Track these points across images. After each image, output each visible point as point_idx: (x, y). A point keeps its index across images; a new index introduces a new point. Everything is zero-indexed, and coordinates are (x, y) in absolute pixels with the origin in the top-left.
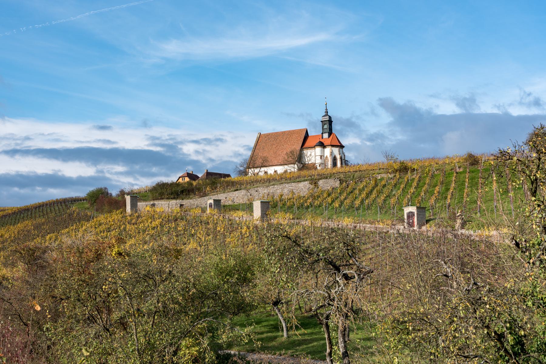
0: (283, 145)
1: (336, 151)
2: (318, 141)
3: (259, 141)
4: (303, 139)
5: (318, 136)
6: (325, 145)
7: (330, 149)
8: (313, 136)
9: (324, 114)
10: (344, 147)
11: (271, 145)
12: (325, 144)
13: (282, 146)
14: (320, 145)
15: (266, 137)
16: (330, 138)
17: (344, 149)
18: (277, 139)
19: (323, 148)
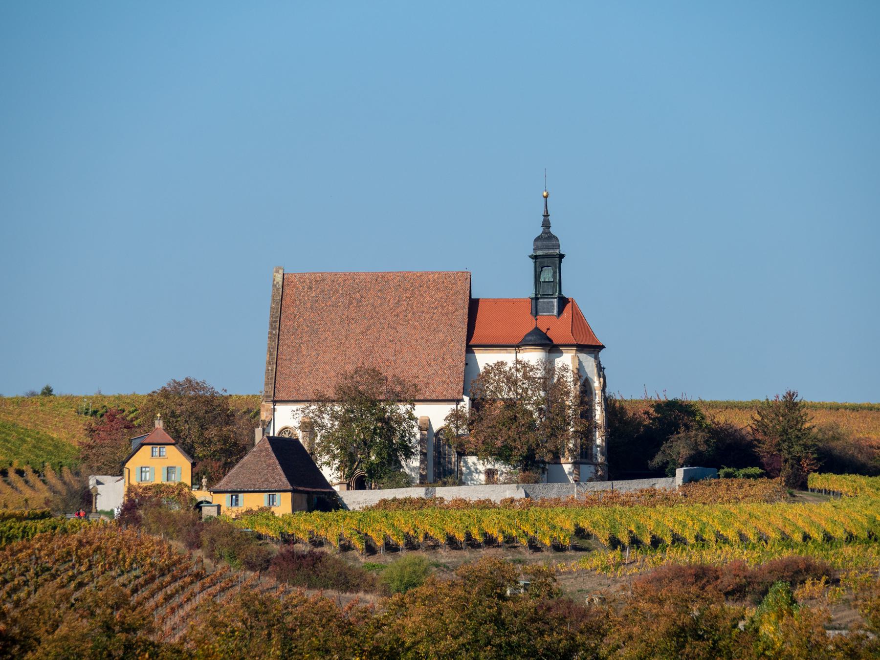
0: (390, 327)
1: (589, 363)
2: (530, 329)
3: (287, 300)
4: (466, 310)
5: (513, 302)
6: (555, 342)
7: (573, 358)
8: (496, 302)
9: (539, 231)
10: (603, 347)
11: (342, 321)
12: (556, 336)
13: (392, 332)
14: (539, 342)
15: (310, 288)
16: (561, 317)
17: (602, 354)
18: (359, 302)
19: (550, 352)
